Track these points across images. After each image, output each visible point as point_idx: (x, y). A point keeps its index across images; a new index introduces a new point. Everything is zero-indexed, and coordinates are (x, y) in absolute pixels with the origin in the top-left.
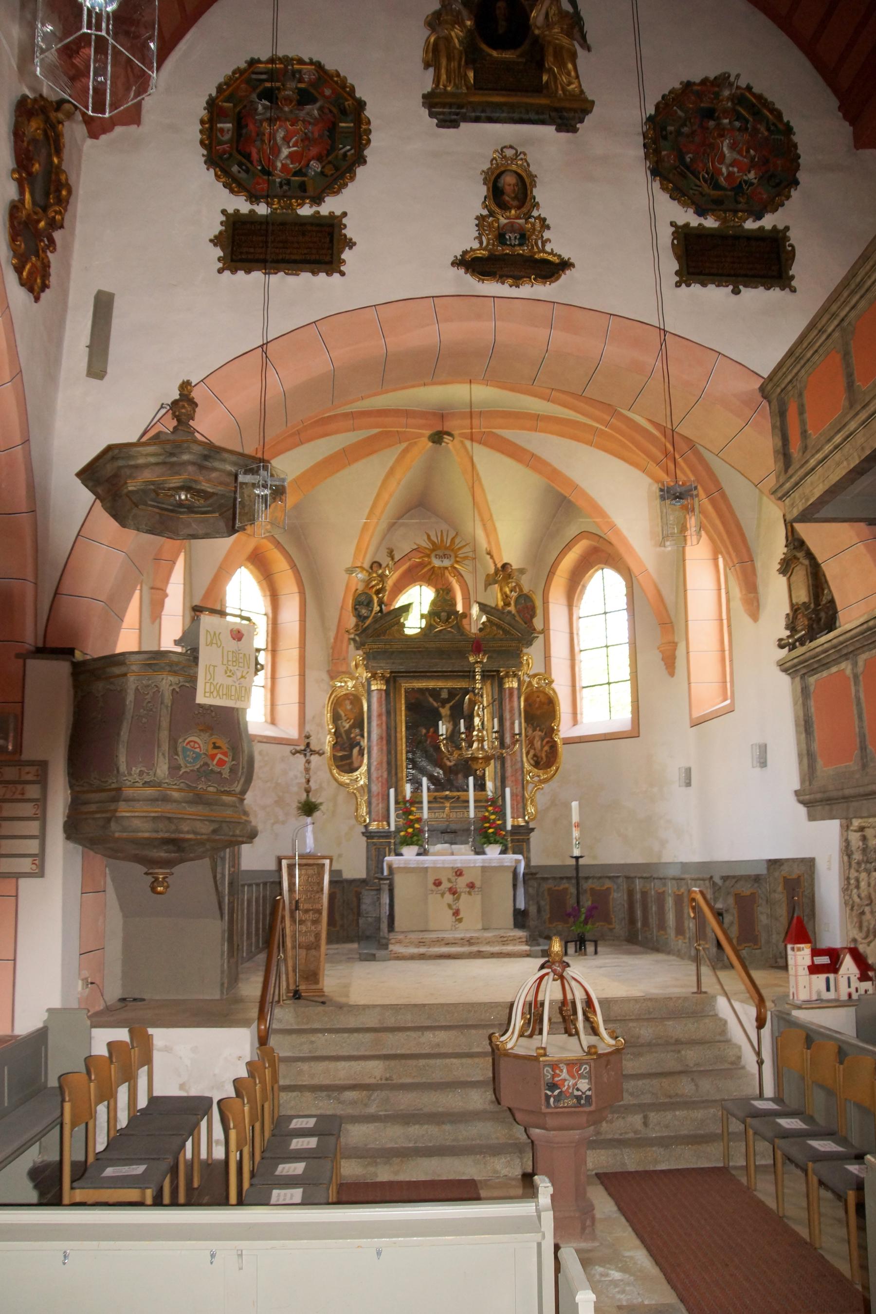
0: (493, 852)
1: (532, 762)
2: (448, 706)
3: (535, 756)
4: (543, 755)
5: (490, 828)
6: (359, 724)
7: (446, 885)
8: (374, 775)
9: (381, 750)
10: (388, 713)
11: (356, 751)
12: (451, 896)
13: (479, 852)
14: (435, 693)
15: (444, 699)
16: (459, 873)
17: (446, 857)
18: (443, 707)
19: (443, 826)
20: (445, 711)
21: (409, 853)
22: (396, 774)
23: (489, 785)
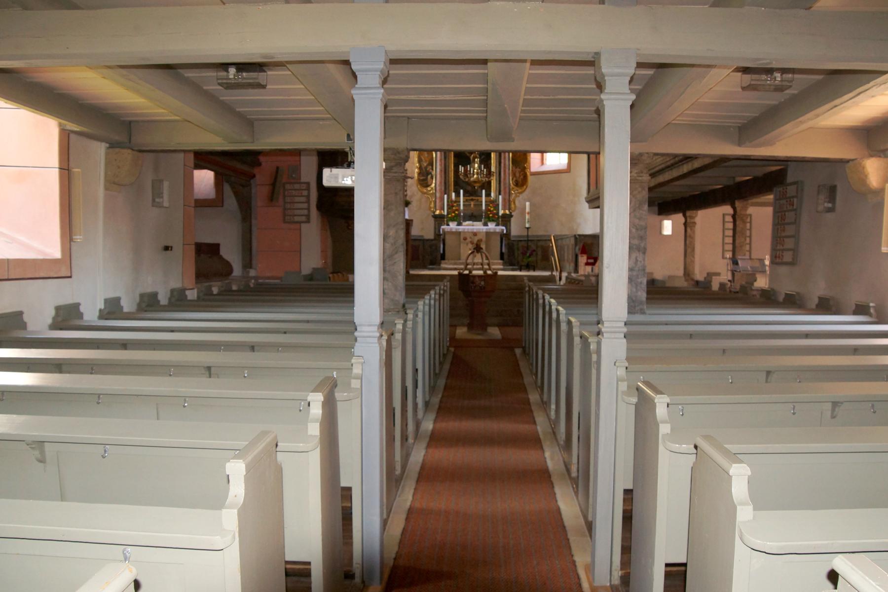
0: (492, 226)
7: (469, 240)
8: (438, 188)
9: (441, 177)
10: (445, 158)
11: (429, 177)
13: (486, 224)
16: (475, 234)
17: (469, 226)
19: (469, 212)
21: (453, 226)
23: (492, 194)
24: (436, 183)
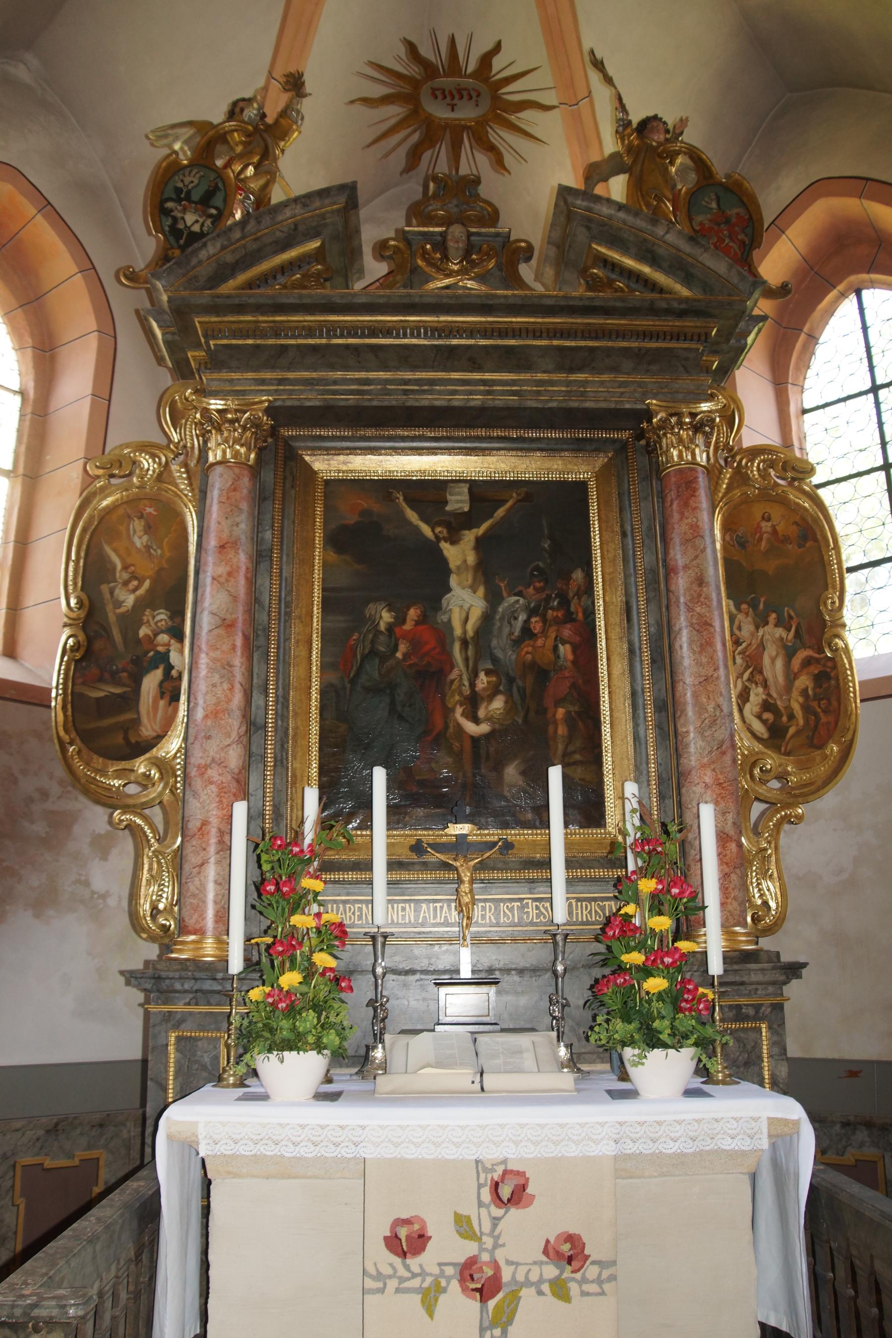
1: (758, 727)
2: (469, 537)
3: (767, 706)
4: (796, 707)
5: (646, 971)
6: (171, 594)
7: (446, 1249)
11: (151, 682)
12: (474, 1305)
14: (427, 493)
15: (457, 515)
16: (510, 1190)
20: (459, 554)
22: (281, 762)
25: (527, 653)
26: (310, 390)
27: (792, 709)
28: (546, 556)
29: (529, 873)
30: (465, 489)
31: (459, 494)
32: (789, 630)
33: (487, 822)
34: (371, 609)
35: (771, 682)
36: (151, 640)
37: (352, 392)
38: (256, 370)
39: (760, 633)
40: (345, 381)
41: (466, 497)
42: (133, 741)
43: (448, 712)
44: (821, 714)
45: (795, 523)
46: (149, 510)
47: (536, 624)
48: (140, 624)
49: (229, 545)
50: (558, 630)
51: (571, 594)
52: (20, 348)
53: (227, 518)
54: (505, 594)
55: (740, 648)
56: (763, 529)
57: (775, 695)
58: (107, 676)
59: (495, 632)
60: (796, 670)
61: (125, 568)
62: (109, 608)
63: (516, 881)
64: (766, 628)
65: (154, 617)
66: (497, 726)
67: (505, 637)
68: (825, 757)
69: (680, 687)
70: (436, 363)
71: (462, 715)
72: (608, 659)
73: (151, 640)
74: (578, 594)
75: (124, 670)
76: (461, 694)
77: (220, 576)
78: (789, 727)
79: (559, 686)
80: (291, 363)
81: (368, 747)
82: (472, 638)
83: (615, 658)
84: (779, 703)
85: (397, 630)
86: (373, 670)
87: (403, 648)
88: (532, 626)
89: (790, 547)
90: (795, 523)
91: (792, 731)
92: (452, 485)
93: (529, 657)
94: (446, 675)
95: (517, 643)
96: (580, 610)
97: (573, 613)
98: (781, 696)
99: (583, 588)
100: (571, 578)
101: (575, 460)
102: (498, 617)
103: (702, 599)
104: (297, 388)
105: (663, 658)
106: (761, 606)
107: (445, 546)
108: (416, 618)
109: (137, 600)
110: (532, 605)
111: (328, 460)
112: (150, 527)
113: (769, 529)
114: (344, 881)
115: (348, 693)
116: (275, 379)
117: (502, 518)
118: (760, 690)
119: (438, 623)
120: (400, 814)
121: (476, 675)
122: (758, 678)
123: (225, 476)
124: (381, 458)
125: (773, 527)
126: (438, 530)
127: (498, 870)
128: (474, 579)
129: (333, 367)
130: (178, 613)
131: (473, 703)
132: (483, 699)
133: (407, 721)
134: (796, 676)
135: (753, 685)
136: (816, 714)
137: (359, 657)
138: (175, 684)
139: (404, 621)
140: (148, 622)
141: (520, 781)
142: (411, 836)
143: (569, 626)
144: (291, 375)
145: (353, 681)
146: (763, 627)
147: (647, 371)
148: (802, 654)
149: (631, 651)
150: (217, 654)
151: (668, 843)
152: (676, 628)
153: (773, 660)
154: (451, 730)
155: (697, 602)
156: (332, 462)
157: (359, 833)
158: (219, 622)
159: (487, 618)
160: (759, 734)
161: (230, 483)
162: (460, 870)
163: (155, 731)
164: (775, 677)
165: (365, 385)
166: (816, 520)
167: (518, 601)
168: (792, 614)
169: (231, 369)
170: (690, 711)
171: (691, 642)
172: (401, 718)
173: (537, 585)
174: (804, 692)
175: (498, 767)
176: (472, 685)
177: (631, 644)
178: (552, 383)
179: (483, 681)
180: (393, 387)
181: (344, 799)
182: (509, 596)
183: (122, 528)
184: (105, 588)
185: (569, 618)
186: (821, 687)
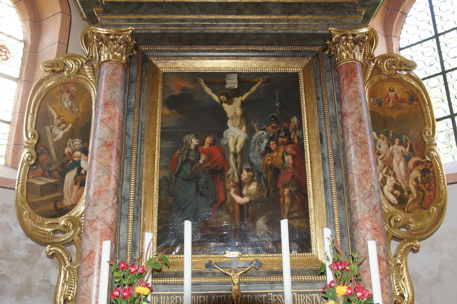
1: (392, 198)
2: (238, 101)
3: (396, 187)
6: (83, 131)
11: (70, 176)
14: (216, 79)
15: (231, 90)
18: (230, 102)
20: (233, 109)
22: (136, 218)
24: (94, 202)
25: (268, 160)
26: (154, 25)
27: (410, 189)
28: (278, 110)
29: (271, 278)
30: (235, 77)
31: (233, 79)
32: (406, 147)
33: (248, 250)
34: (186, 138)
35: (398, 174)
36: (71, 155)
37: (176, 26)
38: (125, 14)
39: (391, 149)
40: (172, 20)
41: (236, 81)
42: (59, 208)
43: (227, 191)
44: (426, 191)
45: (407, 92)
46: (72, 88)
47: (273, 145)
48: (66, 146)
49: (110, 103)
50: (284, 148)
51: (291, 130)
52: (24, 20)
53: (109, 89)
54: (256, 130)
55: (380, 157)
56: (390, 96)
57: (400, 181)
58: (46, 173)
59: (252, 149)
60: (411, 168)
61: (59, 117)
62: (49, 138)
63: (264, 283)
64: (394, 146)
65: (73, 143)
66: (253, 198)
67: (256, 152)
68: (429, 214)
69: (350, 177)
70: (220, 11)
71: (234, 193)
72: (311, 163)
73: (71, 155)
74: (295, 130)
75: (56, 170)
76: (233, 181)
77: (105, 119)
78: (408, 198)
79: (285, 177)
80: (144, 12)
81: (184, 210)
82: (239, 153)
83: (314, 162)
84: (402, 185)
85: (200, 149)
86: (187, 169)
87: (203, 158)
88: (271, 146)
89: (405, 104)
90: (407, 92)
91: (410, 200)
92: (229, 75)
93: (269, 162)
94: (226, 172)
95: (263, 155)
96: (296, 137)
97: (292, 139)
98: (403, 182)
99: (297, 126)
100: (291, 121)
101: (292, 62)
102: (252, 142)
103: (361, 130)
104: (147, 23)
105: (341, 162)
106: (391, 135)
107: (225, 106)
108: (210, 142)
109: (64, 134)
110: (271, 135)
111: (165, 62)
112: (73, 97)
113: (393, 96)
114: (170, 283)
115: (174, 181)
116: (136, 19)
117: (255, 91)
118: (392, 178)
119: (221, 145)
120: (201, 246)
121: (241, 172)
122: (391, 172)
123: (109, 68)
124: (192, 61)
125: (396, 95)
126: (221, 97)
127: (254, 276)
128: (240, 122)
129: (166, 13)
130: (86, 140)
131: (240, 186)
132: (245, 184)
133: (205, 196)
134: (411, 171)
135: (388, 176)
136: (423, 191)
137: (180, 163)
138: (83, 178)
139: (204, 144)
140: (70, 145)
141: (265, 227)
142: (207, 258)
143: (290, 146)
144: (144, 17)
145: (176, 175)
146: (392, 145)
147: (329, 14)
148: (414, 160)
149: (323, 158)
150: (102, 160)
151: (348, 263)
152: (348, 145)
153: (398, 163)
154: (228, 200)
155: (359, 131)
156: (167, 63)
157: (179, 256)
158: (103, 143)
159: (247, 142)
160: (393, 202)
161: (111, 72)
162: (233, 277)
163: (71, 202)
164: (400, 171)
165: (183, 22)
166: (418, 90)
167: (263, 133)
168: (407, 139)
169: (113, 14)
170: (356, 189)
171: (356, 152)
172: (202, 194)
173: (273, 125)
174: (416, 179)
175: (254, 220)
176: (240, 177)
177: (323, 154)
178: (280, 20)
179: (245, 175)
180: (197, 23)
181: (168, 239)
182: (259, 131)
183: (58, 98)
184: (47, 128)
185: (290, 142)
186: (425, 176)
